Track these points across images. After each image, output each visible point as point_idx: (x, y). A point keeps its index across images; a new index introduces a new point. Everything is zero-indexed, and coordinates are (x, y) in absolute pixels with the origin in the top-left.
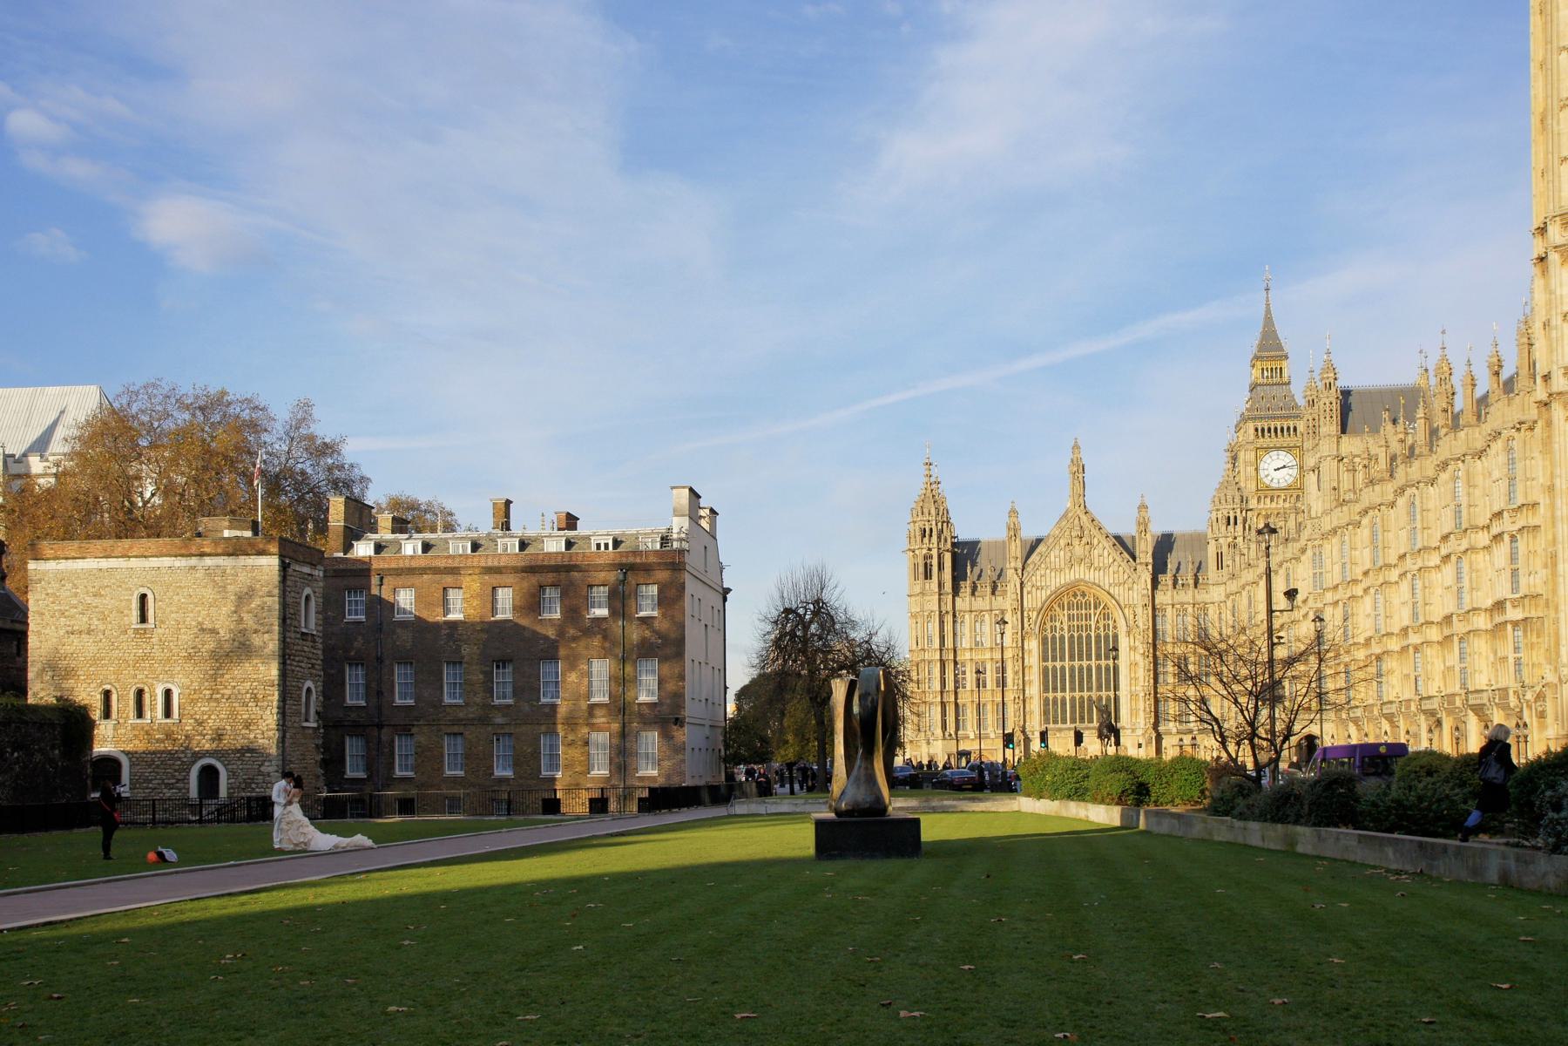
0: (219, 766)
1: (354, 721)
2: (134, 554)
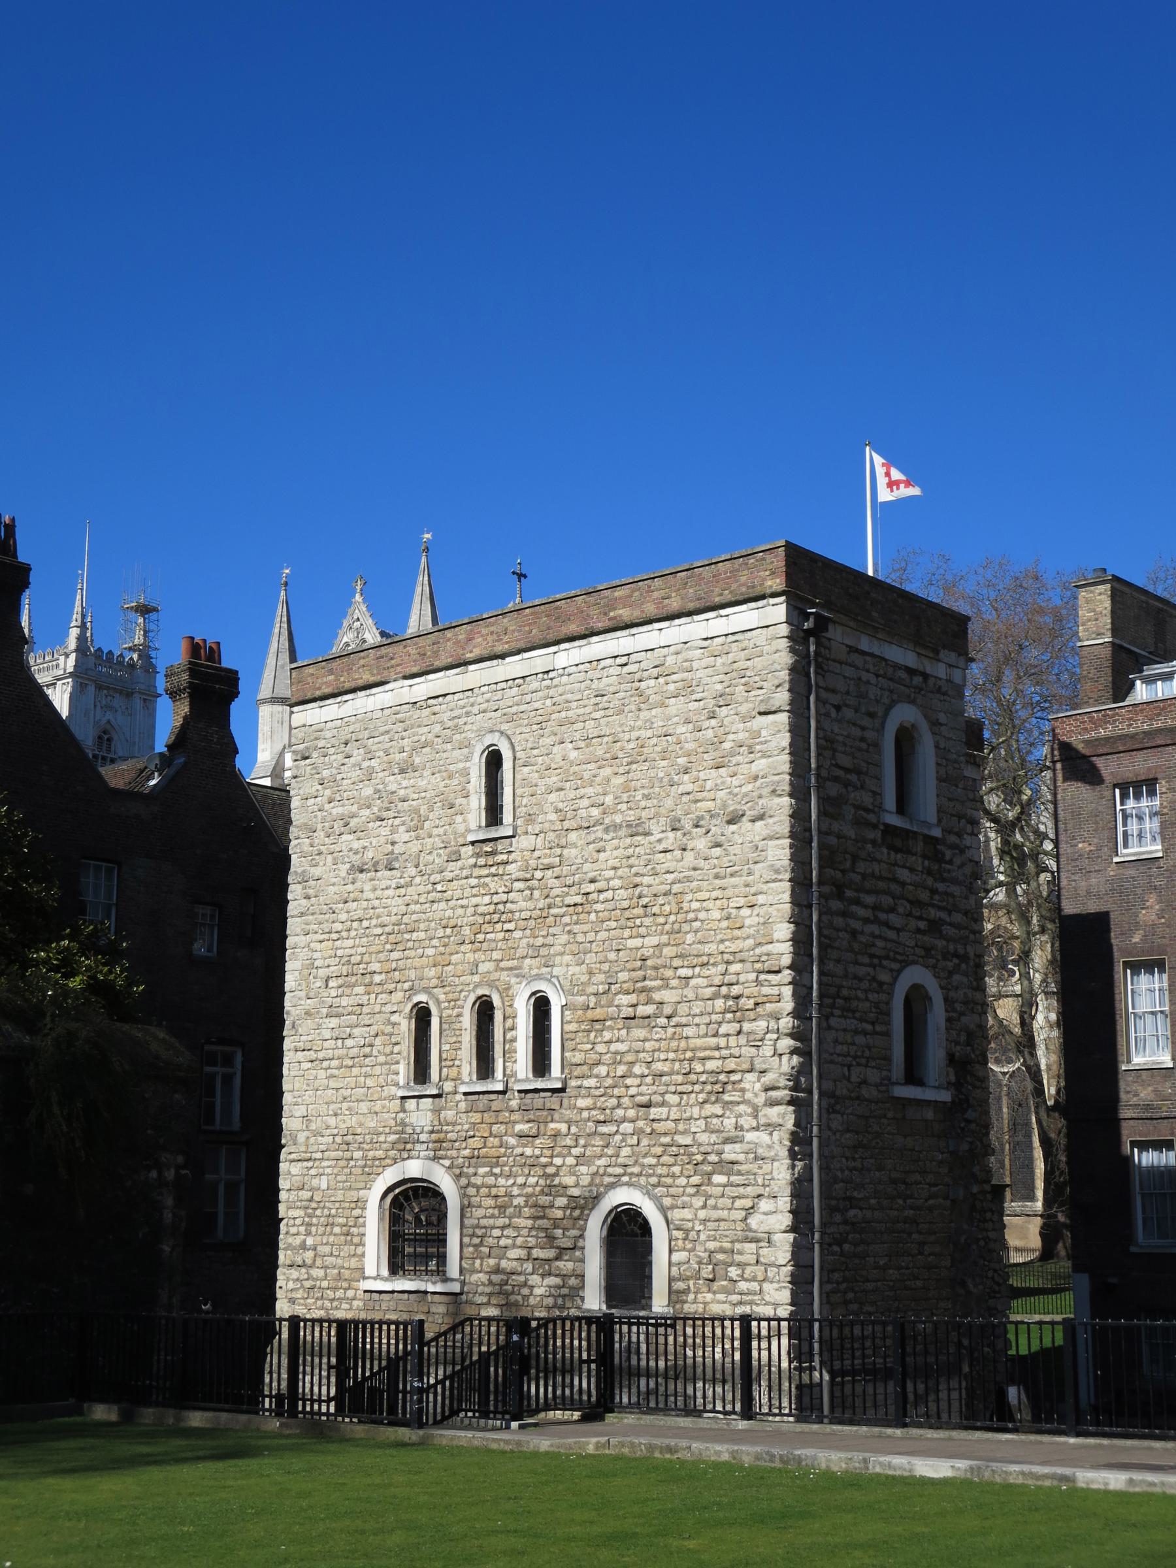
0: (649, 1210)
1: (1148, 1107)
2: (476, 653)
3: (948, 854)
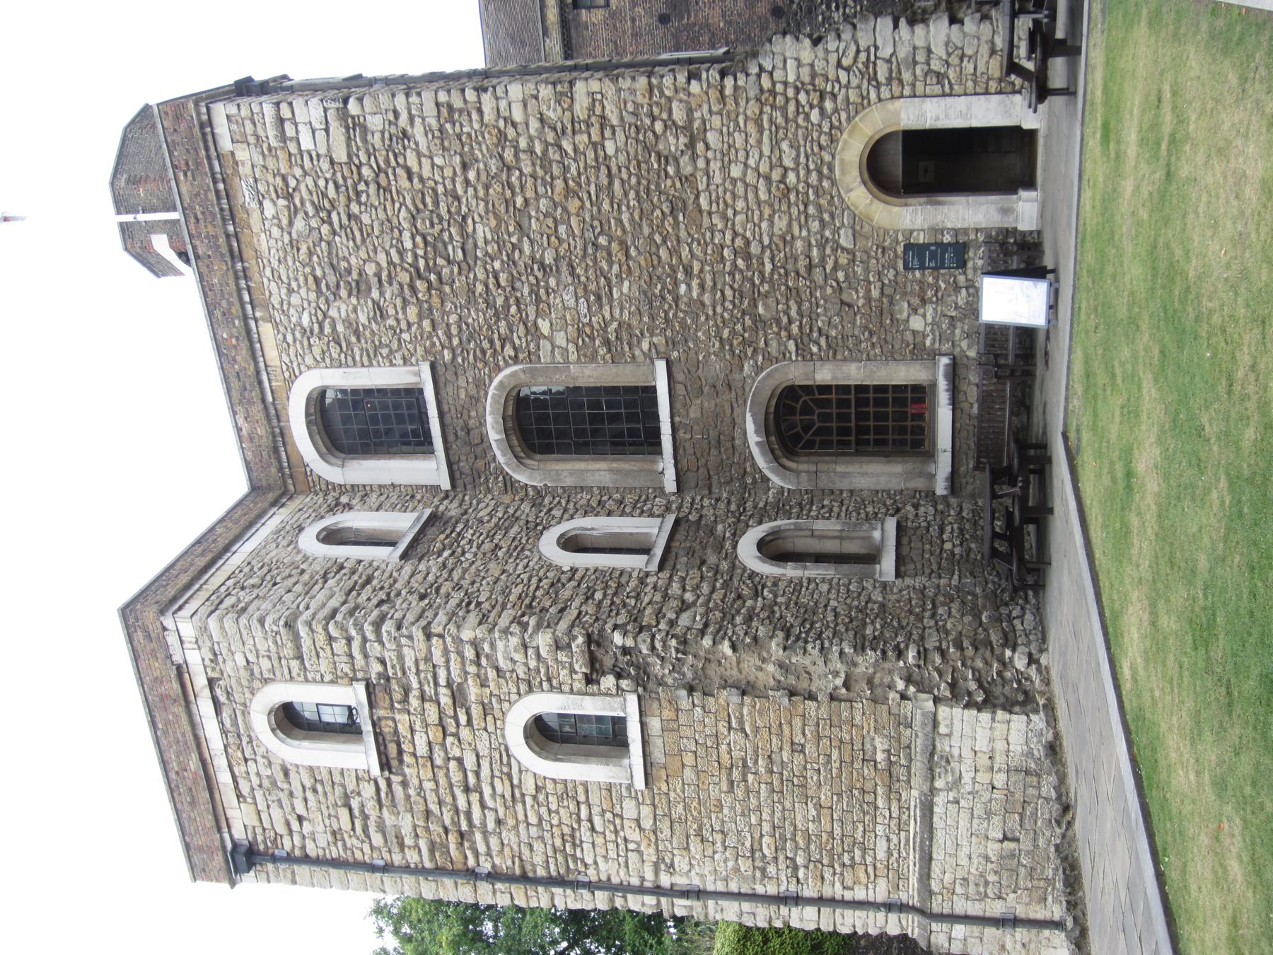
3: (376, 668)
